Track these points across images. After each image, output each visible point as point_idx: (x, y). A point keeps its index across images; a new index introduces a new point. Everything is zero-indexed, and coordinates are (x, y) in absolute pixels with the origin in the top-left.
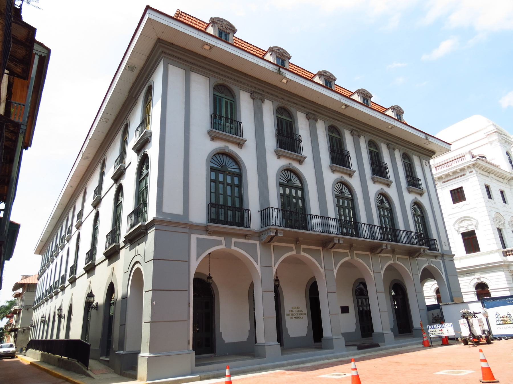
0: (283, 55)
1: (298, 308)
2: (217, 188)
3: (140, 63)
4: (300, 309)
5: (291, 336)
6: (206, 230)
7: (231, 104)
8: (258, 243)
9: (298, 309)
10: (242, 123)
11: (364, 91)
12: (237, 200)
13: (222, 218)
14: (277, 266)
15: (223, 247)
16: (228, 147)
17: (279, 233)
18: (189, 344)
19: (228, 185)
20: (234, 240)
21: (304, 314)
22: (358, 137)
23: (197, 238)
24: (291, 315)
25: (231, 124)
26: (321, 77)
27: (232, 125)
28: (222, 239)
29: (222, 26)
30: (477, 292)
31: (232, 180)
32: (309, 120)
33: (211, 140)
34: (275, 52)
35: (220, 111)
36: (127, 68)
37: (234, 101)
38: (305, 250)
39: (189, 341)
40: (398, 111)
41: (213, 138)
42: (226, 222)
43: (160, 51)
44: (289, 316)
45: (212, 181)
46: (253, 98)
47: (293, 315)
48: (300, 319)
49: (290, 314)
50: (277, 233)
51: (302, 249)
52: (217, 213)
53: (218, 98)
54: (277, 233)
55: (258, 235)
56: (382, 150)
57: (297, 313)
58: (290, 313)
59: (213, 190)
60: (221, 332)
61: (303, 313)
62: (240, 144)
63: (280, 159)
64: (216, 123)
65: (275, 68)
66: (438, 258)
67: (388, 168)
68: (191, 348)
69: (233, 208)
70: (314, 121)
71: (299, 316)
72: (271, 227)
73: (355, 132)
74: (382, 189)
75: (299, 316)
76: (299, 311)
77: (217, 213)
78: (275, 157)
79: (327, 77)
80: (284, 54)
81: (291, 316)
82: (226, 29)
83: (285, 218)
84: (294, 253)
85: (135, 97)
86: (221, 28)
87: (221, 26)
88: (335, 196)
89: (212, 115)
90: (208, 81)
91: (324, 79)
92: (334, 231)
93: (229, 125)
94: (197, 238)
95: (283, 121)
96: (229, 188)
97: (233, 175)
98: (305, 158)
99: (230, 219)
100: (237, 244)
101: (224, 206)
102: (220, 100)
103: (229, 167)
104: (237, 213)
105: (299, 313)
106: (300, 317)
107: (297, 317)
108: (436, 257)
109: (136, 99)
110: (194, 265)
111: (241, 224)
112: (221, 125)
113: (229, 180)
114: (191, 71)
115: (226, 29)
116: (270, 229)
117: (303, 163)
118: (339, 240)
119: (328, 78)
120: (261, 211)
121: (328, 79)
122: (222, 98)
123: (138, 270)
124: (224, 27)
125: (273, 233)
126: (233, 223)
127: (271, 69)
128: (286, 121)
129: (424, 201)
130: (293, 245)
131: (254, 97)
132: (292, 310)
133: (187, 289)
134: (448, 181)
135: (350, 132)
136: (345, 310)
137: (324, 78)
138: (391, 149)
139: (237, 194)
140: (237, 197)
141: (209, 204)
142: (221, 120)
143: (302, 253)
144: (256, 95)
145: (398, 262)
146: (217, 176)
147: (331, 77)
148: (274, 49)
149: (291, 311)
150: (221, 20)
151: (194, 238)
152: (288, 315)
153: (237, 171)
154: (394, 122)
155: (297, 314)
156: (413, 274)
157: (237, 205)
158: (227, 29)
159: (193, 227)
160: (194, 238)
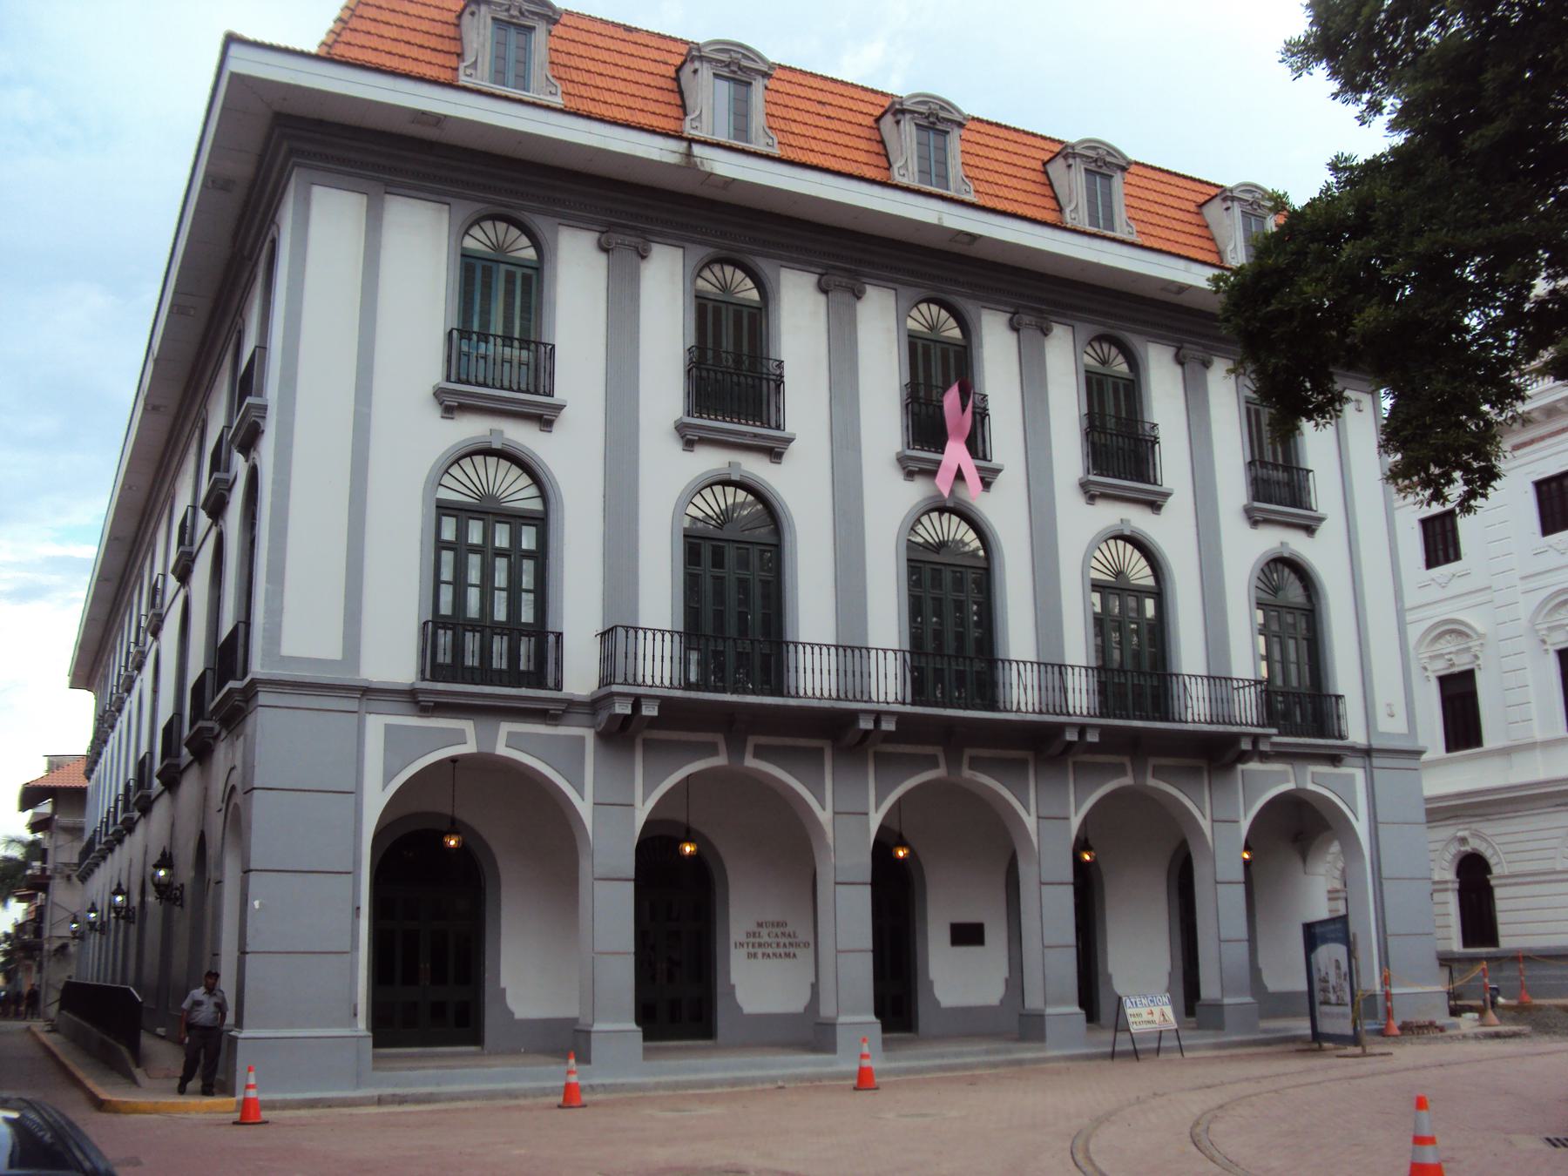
0: (740, 68)
1: (778, 924)
2: (460, 569)
3: (241, 169)
4: (787, 930)
6: (412, 699)
7: (527, 280)
8: (589, 735)
9: (779, 930)
10: (553, 346)
11: (1094, 148)
12: (527, 600)
13: (471, 660)
14: (651, 803)
15: (469, 748)
16: (501, 432)
17: (644, 707)
18: (355, 1015)
19: (501, 553)
20: (506, 728)
22: (1039, 332)
23: (388, 727)
25: (521, 348)
26: (902, 122)
27: (525, 353)
28: (467, 726)
29: (508, 10)
30: (1461, 883)
31: (515, 538)
32: (830, 295)
33: (442, 417)
34: (710, 60)
35: (486, 313)
36: (210, 184)
37: (536, 269)
38: (760, 752)
39: (356, 1007)
40: (1251, 205)
41: (451, 405)
42: (485, 674)
43: (285, 146)
44: (743, 952)
45: (441, 545)
46: (604, 248)
47: (760, 945)
48: (788, 960)
50: (636, 706)
51: (750, 749)
52: (458, 649)
53: (479, 265)
54: (636, 706)
55: (594, 705)
56: (1147, 369)
57: (776, 940)
59: (447, 575)
60: (504, 990)
61: (797, 940)
62: (544, 419)
63: (692, 451)
64: (468, 355)
65: (675, 149)
66: (1347, 760)
67: (1161, 440)
68: (362, 1025)
69: (513, 629)
70: (847, 297)
71: (782, 950)
72: (615, 688)
73: (1026, 319)
74: (1122, 520)
75: (782, 950)
77: (458, 649)
78: (676, 447)
79: (927, 117)
80: (745, 63)
81: (751, 950)
82: (522, 13)
83: (698, 649)
84: (720, 760)
85: (250, 259)
86: (503, 16)
87: (504, 8)
88: (909, 560)
89: (450, 333)
90: (445, 216)
91: (914, 128)
92: (862, 692)
93: (516, 352)
94: (388, 727)
95: (724, 312)
96: (501, 564)
97: (517, 519)
98: (789, 441)
99: (499, 662)
100: (512, 741)
101: (486, 627)
102: (488, 274)
103: (505, 495)
104: (526, 646)
105: (787, 941)
106: (787, 955)
107: (774, 954)
108: (1334, 759)
109: (254, 260)
110: (375, 802)
111: (537, 678)
112: (485, 357)
113: (502, 538)
114: (386, 193)
115: (522, 13)
116: (612, 695)
117: (784, 456)
118: (877, 722)
119: (931, 119)
120: (603, 634)
121: (931, 123)
122: (494, 266)
123: (236, 804)
124: (514, 12)
125: (622, 708)
126: (513, 676)
127: (655, 155)
128: (738, 308)
129: (1313, 551)
130: (719, 739)
131: (609, 244)
132: (760, 929)
133: (350, 869)
134: (1532, 442)
135: (1009, 315)
136: (968, 935)
137: (916, 124)
138: (1192, 363)
139: (527, 581)
140: (528, 591)
141: (426, 623)
142: (487, 342)
143: (751, 762)
144: (616, 238)
145: (1152, 782)
146: (462, 531)
147: (943, 114)
148: (706, 52)
153: (536, 505)
154: (1187, 271)
155: (774, 945)
156: (1213, 821)
157: (527, 615)
158: (527, 14)
159: (368, 693)
160: (376, 725)
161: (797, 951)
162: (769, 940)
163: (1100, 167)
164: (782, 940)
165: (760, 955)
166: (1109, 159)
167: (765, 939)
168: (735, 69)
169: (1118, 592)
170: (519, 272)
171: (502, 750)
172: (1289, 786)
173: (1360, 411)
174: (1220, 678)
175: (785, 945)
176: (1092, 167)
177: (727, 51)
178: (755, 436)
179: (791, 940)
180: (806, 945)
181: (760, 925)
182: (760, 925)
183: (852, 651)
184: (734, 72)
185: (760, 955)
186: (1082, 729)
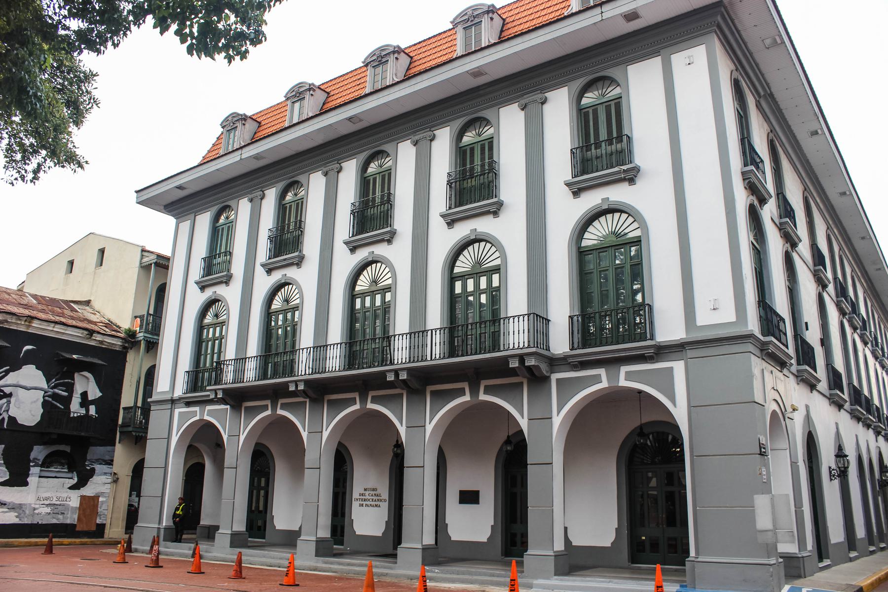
1: (374, 490)
5: (359, 532)
9: (374, 493)
21: (383, 500)
23: (180, 413)
24: (362, 501)
44: (358, 503)
47: (365, 501)
49: (360, 499)
58: (360, 497)
76: (375, 495)
81: (362, 503)
82: (234, 123)
106: (376, 506)
118: (297, 386)
121: (380, 61)
124: (232, 124)
132: (364, 492)
136: (469, 497)
143: (280, 412)
149: (363, 495)
150: (226, 119)
151: (177, 411)
152: (357, 499)
155: (371, 500)
159: (173, 402)
161: (380, 503)
162: (369, 498)
163: (472, 21)
164: (375, 498)
165: (364, 505)
166: (476, 13)
167: (367, 497)
168: (298, 95)
169: (461, 278)
170: (231, 224)
171: (206, 418)
172: (604, 384)
173: (689, 64)
174: (540, 317)
175: (375, 500)
176: (469, 24)
177: (294, 91)
178: (285, 260)
179: (379, 498)
180: (385, 501)
181: (365, 490)
182: (365, 490)
183: (321, 348)
184: (298, 97)
185: (364, 505)
186: (396, 373)
